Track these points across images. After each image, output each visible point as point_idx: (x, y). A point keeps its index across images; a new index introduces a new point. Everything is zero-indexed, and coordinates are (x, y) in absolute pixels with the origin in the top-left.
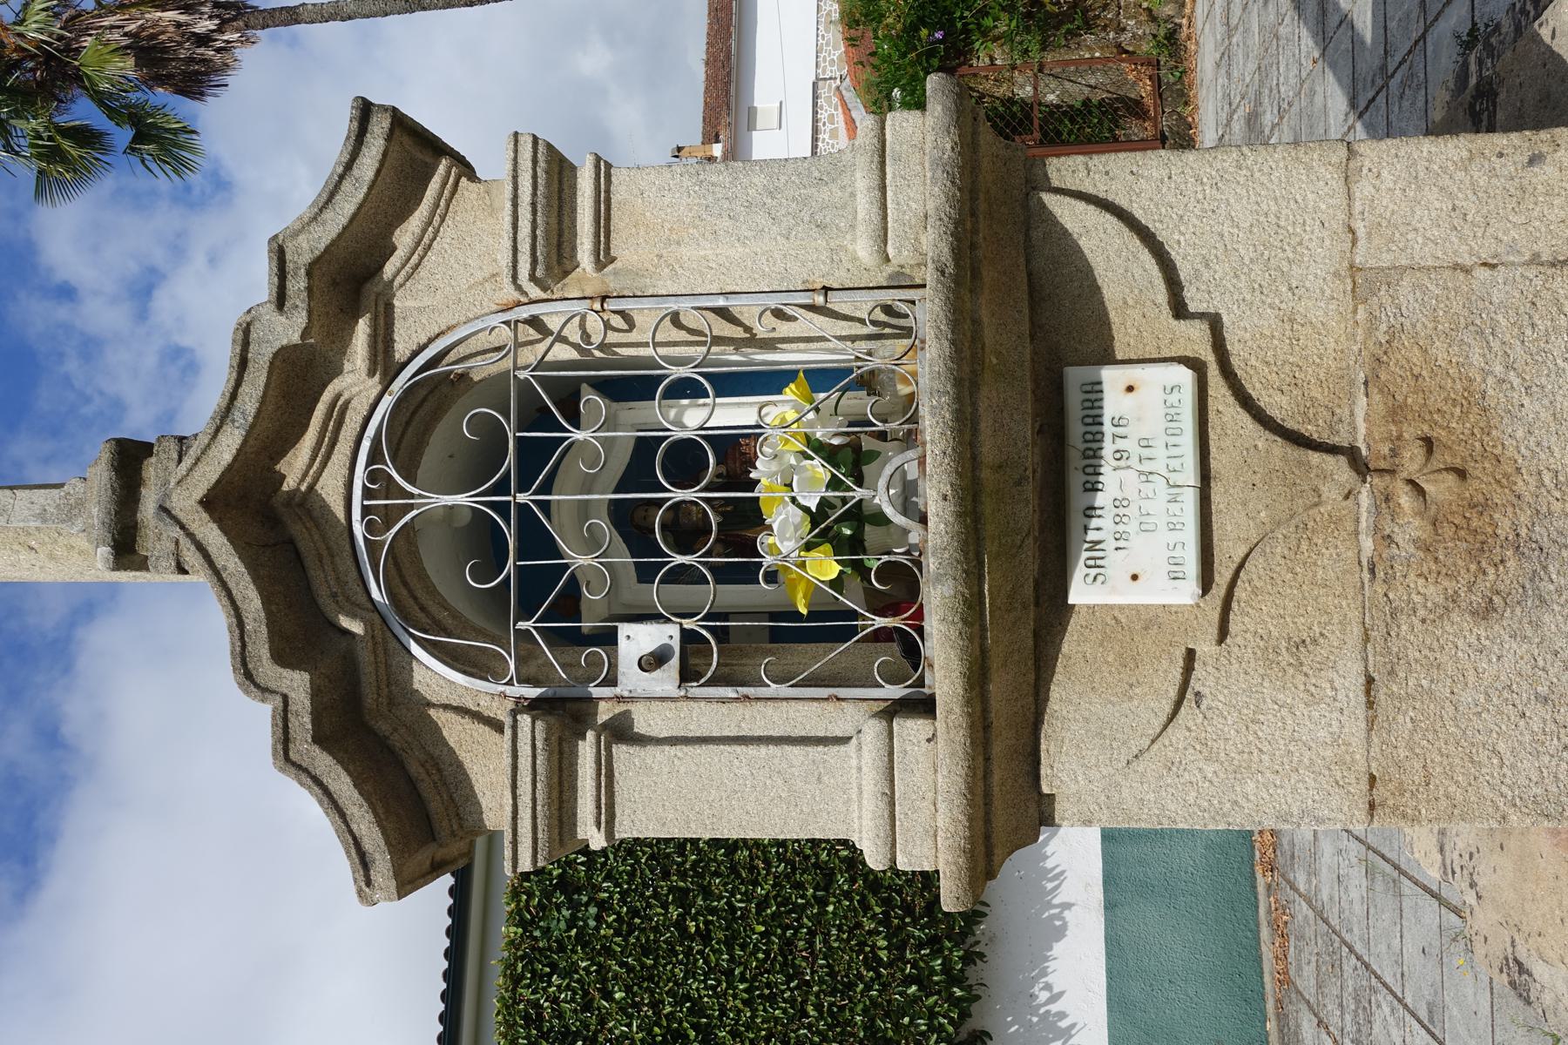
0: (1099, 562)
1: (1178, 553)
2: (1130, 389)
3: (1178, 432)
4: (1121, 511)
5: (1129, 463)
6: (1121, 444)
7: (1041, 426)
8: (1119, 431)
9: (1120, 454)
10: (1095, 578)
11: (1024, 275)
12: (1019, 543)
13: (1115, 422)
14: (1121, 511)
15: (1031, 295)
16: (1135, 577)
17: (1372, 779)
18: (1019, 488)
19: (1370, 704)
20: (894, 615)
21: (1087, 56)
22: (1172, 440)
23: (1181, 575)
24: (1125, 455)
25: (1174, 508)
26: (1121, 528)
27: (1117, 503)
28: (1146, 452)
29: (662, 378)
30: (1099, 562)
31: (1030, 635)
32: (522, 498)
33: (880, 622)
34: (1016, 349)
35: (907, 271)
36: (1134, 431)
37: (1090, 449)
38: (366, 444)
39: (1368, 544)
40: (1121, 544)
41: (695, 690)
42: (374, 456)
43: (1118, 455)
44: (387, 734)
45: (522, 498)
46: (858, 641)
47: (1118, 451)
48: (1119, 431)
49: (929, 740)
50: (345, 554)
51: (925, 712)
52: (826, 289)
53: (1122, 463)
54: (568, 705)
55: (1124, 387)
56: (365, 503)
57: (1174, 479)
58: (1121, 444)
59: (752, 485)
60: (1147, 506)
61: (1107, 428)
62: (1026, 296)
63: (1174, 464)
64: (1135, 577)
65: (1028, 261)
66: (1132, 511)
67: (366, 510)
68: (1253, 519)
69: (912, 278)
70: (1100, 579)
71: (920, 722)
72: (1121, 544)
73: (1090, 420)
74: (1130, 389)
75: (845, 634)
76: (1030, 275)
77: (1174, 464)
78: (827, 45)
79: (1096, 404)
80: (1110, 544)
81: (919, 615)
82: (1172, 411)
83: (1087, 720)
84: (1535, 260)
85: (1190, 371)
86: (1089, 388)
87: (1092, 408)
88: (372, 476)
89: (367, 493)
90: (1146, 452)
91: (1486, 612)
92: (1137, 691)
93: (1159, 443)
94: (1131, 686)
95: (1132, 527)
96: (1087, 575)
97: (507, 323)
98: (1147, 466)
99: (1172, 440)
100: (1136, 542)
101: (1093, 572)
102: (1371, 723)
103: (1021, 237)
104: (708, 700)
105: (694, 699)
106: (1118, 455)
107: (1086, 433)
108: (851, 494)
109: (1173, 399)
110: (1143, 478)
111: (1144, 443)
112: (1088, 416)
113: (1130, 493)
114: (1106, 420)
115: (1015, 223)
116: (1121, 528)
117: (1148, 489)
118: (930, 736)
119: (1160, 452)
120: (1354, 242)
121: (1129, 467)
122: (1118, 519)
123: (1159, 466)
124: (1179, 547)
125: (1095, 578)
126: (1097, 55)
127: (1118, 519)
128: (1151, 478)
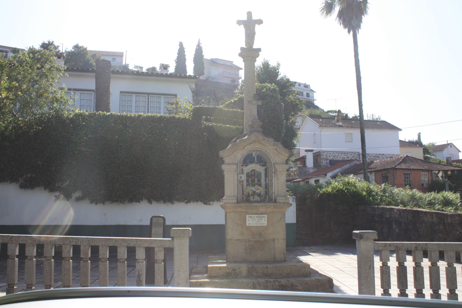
16: (249, 220)
17: (231, 240)
19: (238, 240)
21: (332, 225)
29: (267, 178)
33: (245, 198)
38: (262, 150)
39: (251, 240)
42: (261, 151)
52: (274, 194)
61: (261, 218)
67: (255, 150)
76: (275, 212)
78: (370, 157)
84: (275, 254)
88: (258, 150)
89: (256, 150)
91: (245, 249)
102: (236, 240)
120: (277, 239)
126: (332, 227)
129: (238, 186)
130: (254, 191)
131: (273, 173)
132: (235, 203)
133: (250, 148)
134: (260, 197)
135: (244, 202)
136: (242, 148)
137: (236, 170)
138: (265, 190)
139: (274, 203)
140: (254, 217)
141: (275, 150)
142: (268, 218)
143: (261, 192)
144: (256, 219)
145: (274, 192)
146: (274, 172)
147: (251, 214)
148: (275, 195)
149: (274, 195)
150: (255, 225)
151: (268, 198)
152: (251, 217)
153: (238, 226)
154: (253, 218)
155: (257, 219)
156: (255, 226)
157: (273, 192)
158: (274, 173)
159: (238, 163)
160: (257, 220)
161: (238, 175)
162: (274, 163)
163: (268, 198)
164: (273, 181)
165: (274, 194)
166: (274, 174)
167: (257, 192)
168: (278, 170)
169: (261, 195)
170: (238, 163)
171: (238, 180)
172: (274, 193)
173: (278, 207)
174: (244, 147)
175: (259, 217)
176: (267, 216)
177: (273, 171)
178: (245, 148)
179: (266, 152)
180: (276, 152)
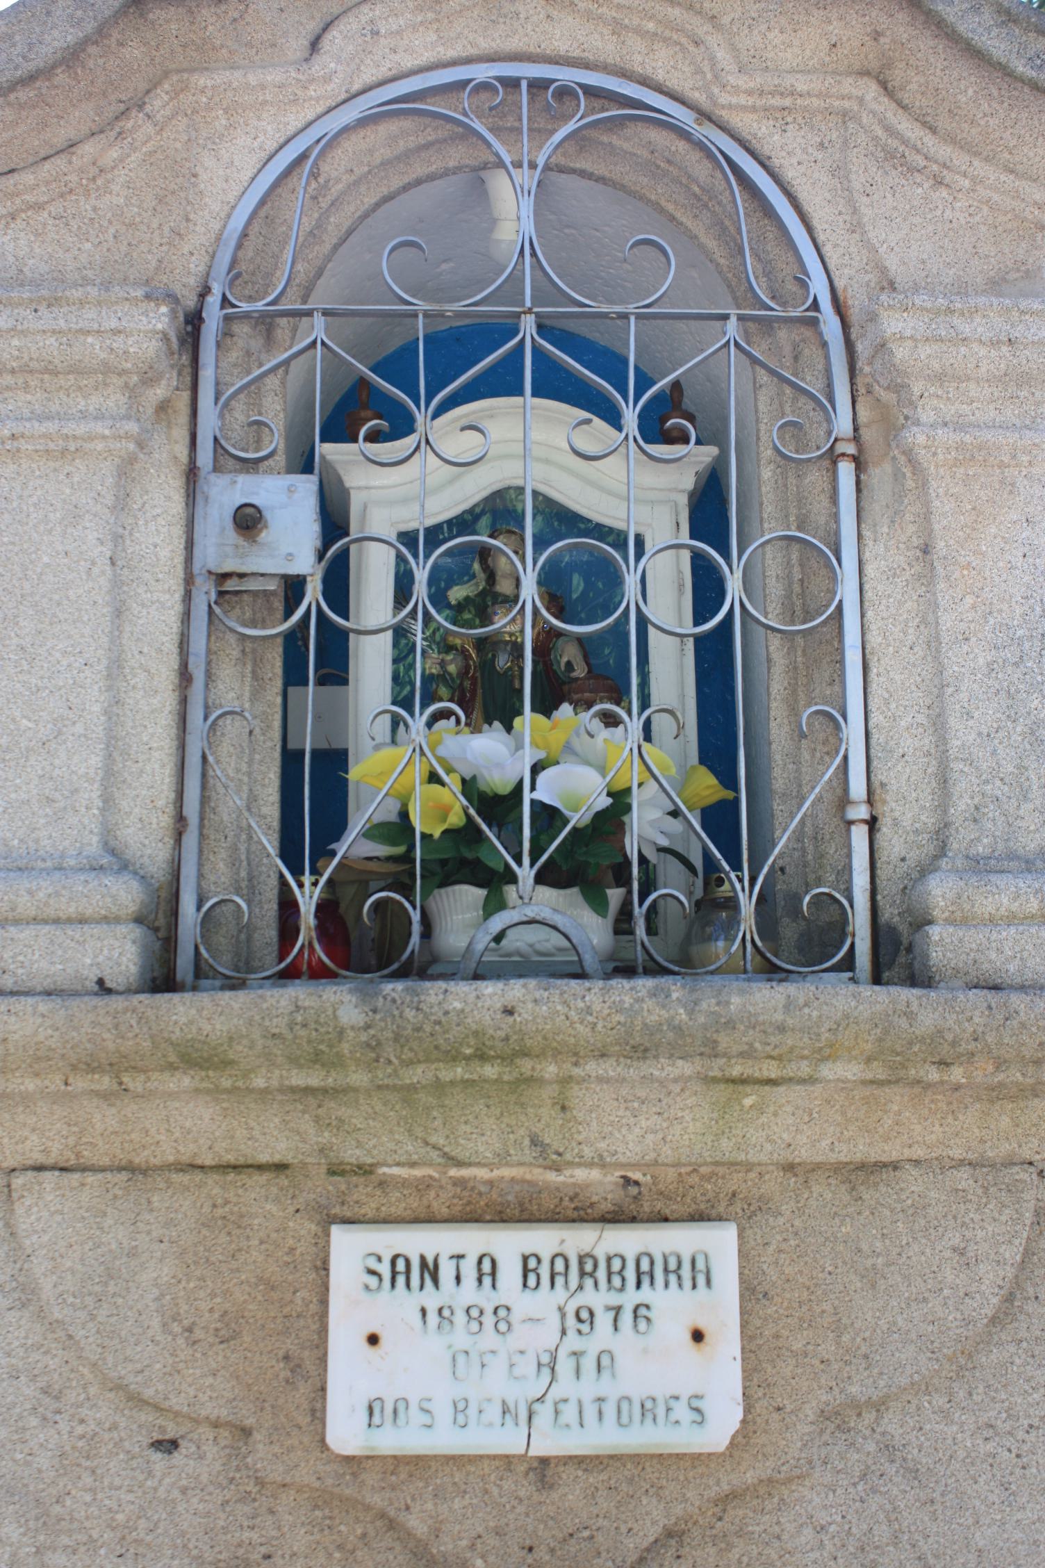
0: (401, 1280)
1: (415, 1414)
2: (698, 1336)
3: (625, 1420)
4: (489, 1320)
5: (571, 1333)
6: (604, 1320)
7: (637, 1183)
8: (627, 1317)
9: (586, 1317)
10: (372, 1272)
11: (894, 1156)
12: (433, 1139)
13: (643, 1311)
14: (489, 1320)
15: (862, 1166)
16: (373, 1340)
18: (527, 1142)
20: (321, 929)
22: (610, 1410)
23: (376, 1419)
24: (585, 1328)
25: (494, 1412)
26: (460, 1318)
27: (502, 1313)
28: (589, 1364)
29: (726, 553)
30: (401, 1280)
31: (277, 1158)
32: (528, 325)
34: (769, 1139)
35: (902, 959)
36: (625, 1343)
37: (596, 1266)
40: (432, 1318)
41: (205, 593)
43: (584, 1315)
44: (148, 108)
45: (528, 325)
46: (282, 876)
47: (592, 1314)
48: (627, 1317)
49: (101, 982)
50: (441, 49)
51: (154, 980)
52: (872, 823)
53: (571, 1321)
54: (186, 395)
55: (702, 1325)
56: (524, 84)
57: (544, 1413)
58: (604, 1320)
59: (545, 706)
60: (498, 1366)
61: (631, 1298)
62: (859, 1157)
63: (569, 1413)
64: (373, 1340)
65: (917, 1162)
66: (489, 1339)
67: (512, 84)
68: (472, 1547)
69: (890, 966)
70: (373, 1281)
71: (134, 969)
72: (432, 1318)
73: (645, 1266)
74: (698, 1336)
75: (290, 852)
76: (895, 1166)
77: (569, 1413)
79: (673, 1278)
80: (431, 1298)
81: (319, 973)
82: (661, 1411)
83: (133, 1253)
85: (726, 1442)
86: (700, 1265)
87: (666, 1270)
88: (564, 93)
89: (538, 85)
90: (589, 1364)
92: (180, 1341)
93: (609, 1388)
94: (190, 1330)
95: (460, 1335)
96: (379, 1259)
97: (815, 306)
98: (565, 1366)
99: (610, 1410)
100: (435, 1345)
101: (385, 1269)
103: (957, 1153)
104: (186, 617)
105: (188, 597)
106: (584, 1315)
107: (623, 1260)
108: (526, 860)
109: (681, 1411)
110: (545, 1359)
111: (605, 1361)
112: (652, 1263)
113: (522, 1336)
114: (646, 1294)
115: (983, 1141)
116: (460, 1318)
117: (527, 1367)
118: (109, 984)
119: (588, 1387)
121: (564, 1332)
122: (474, 1313)
123: (565, 1385)
124: (426, 1419)
125: (372, 1272)
127: (474, 1313)
128: (546, 1372)
129: (185, 677)
130: (499, 781)
131: (833, 457)
132: (103, 988)
133: (426, 57)
134: (615, 895)
135: (289, 974)
136: (297, 45)
137: (163, 407)
138: (707, 786)
139: (877, 980)
140: (488, 1270)
141: (864, 73)
142: (751, 1291)
143: (620, 800)
144: (524, 1303)
145: (858, 788)
146: (856, 438)
147: (428, 1219)
148: (893, 844)
149: (859, 836)
150: (509, 1441)
151: (747, 907)
152: (430, 1270)
153: (169, 1446)
154: (469, 1293)
155: (545, 1302)
156: (507, 1461)
157: (844, 801)
158: (859, 463)
159: (205, 292)
160: (547, 1335)
161: (192, 474)
162: (856, 303)
163: (747, 907)
164: (848, 592)
165: (872, 823)
166: (846, 470)
167: (547, 790)
168: (927, 416)
169: (621, 875)
170: (217, 290)
171: (189, 580)
172: (862, 812)
173: (957, 1074)
174: (326, 28)
175: (587, 1266)
176: (743, 1254)
177: (843, 424)
178: (334, 40)
179: (705, 116)
180: (885, 106)
